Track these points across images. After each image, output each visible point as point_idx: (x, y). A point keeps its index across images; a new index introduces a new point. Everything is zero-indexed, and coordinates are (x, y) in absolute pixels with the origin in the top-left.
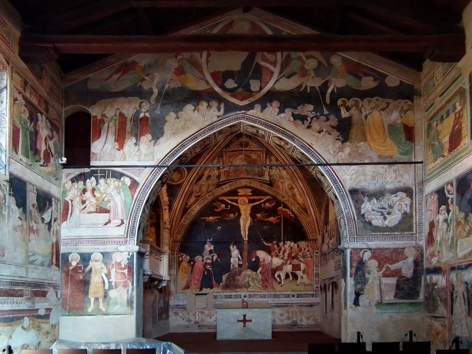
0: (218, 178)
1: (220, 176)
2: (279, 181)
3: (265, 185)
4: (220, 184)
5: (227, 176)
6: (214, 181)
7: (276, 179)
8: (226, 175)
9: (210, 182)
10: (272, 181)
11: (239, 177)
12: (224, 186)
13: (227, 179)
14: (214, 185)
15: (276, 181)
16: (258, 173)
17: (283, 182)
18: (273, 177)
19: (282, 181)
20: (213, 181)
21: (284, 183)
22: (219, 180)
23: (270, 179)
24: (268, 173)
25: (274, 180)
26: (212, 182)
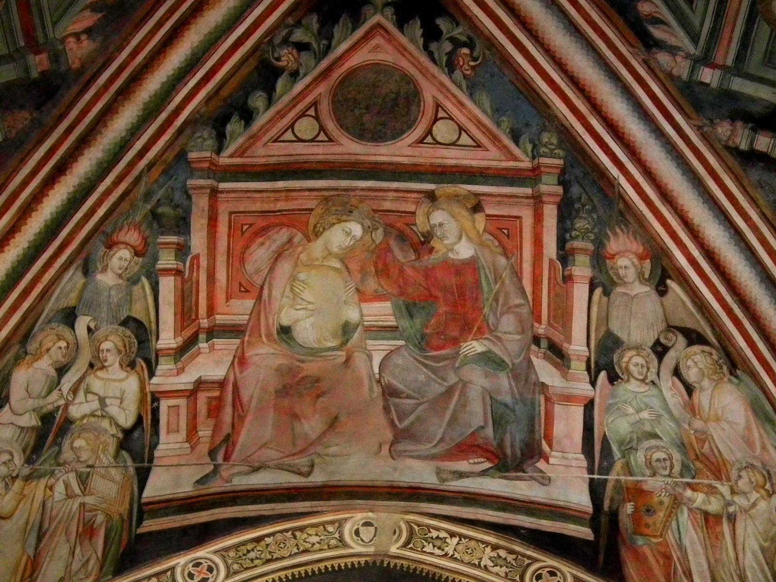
0: (136, 457)
1: (154, 446)
2: (677, 502)
3: (551, 562)
4: (151, 525)
5: (212, 453)
6: (98, 483)
7: (652, 484)
8: (205, 432)
9: (60, 488)
10: (614, 516)
11: (318, 478)
12: (181, 561)
13: (216, 486)
14: (88, 531)
15: (649, 511)
16: (489, 431)
17: (718, 518)
18: (628, 470)
19: (714, 506)
20: (84, 480)
21: (732, 519)
22: (143, 476)
23: (596, 490)
24: (578, 412)
25: (637, 493)
26: (70, 496)
